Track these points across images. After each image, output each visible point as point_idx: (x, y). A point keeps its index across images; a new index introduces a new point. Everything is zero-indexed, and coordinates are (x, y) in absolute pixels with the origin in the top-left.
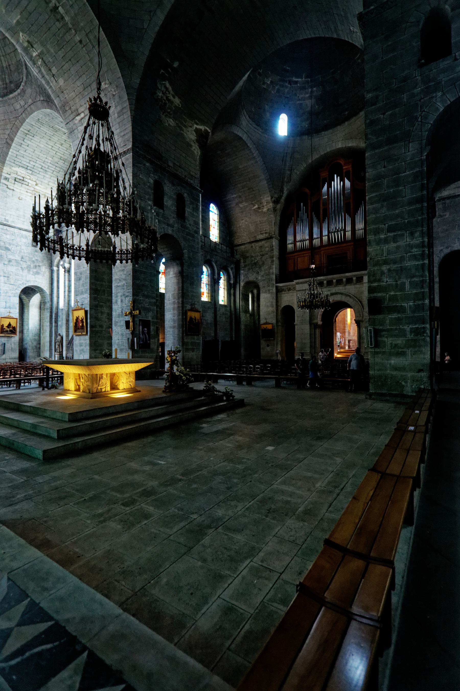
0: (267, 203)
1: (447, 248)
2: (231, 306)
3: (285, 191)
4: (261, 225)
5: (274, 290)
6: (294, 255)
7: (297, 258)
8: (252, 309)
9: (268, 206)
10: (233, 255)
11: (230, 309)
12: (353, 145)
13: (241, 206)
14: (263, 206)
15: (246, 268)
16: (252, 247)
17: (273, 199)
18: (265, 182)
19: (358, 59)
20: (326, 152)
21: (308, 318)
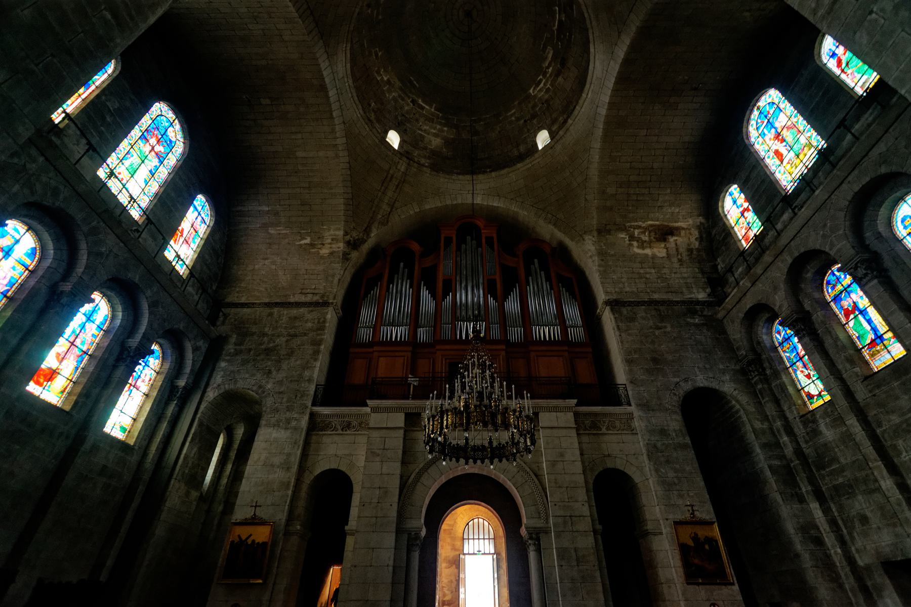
0: (332, 240)
1: (686, 380)
2: (145, 454)
3: (372, 235)
4: (306, 277)
5: (304, 422)
6: (371, 350)
7: (379, 357)
8: (212, 480)
9: (334, 246)
10: (213, 320)
11: (141, 463)
12: (499, 205)
13: (273, 232)
14: (323, 244)
15: (239, 358)
16: (271, 314)
17: (348, 238)
18: (342, 201)
19: (512, 115)
20: (455, 202)
21: (394, 513)
